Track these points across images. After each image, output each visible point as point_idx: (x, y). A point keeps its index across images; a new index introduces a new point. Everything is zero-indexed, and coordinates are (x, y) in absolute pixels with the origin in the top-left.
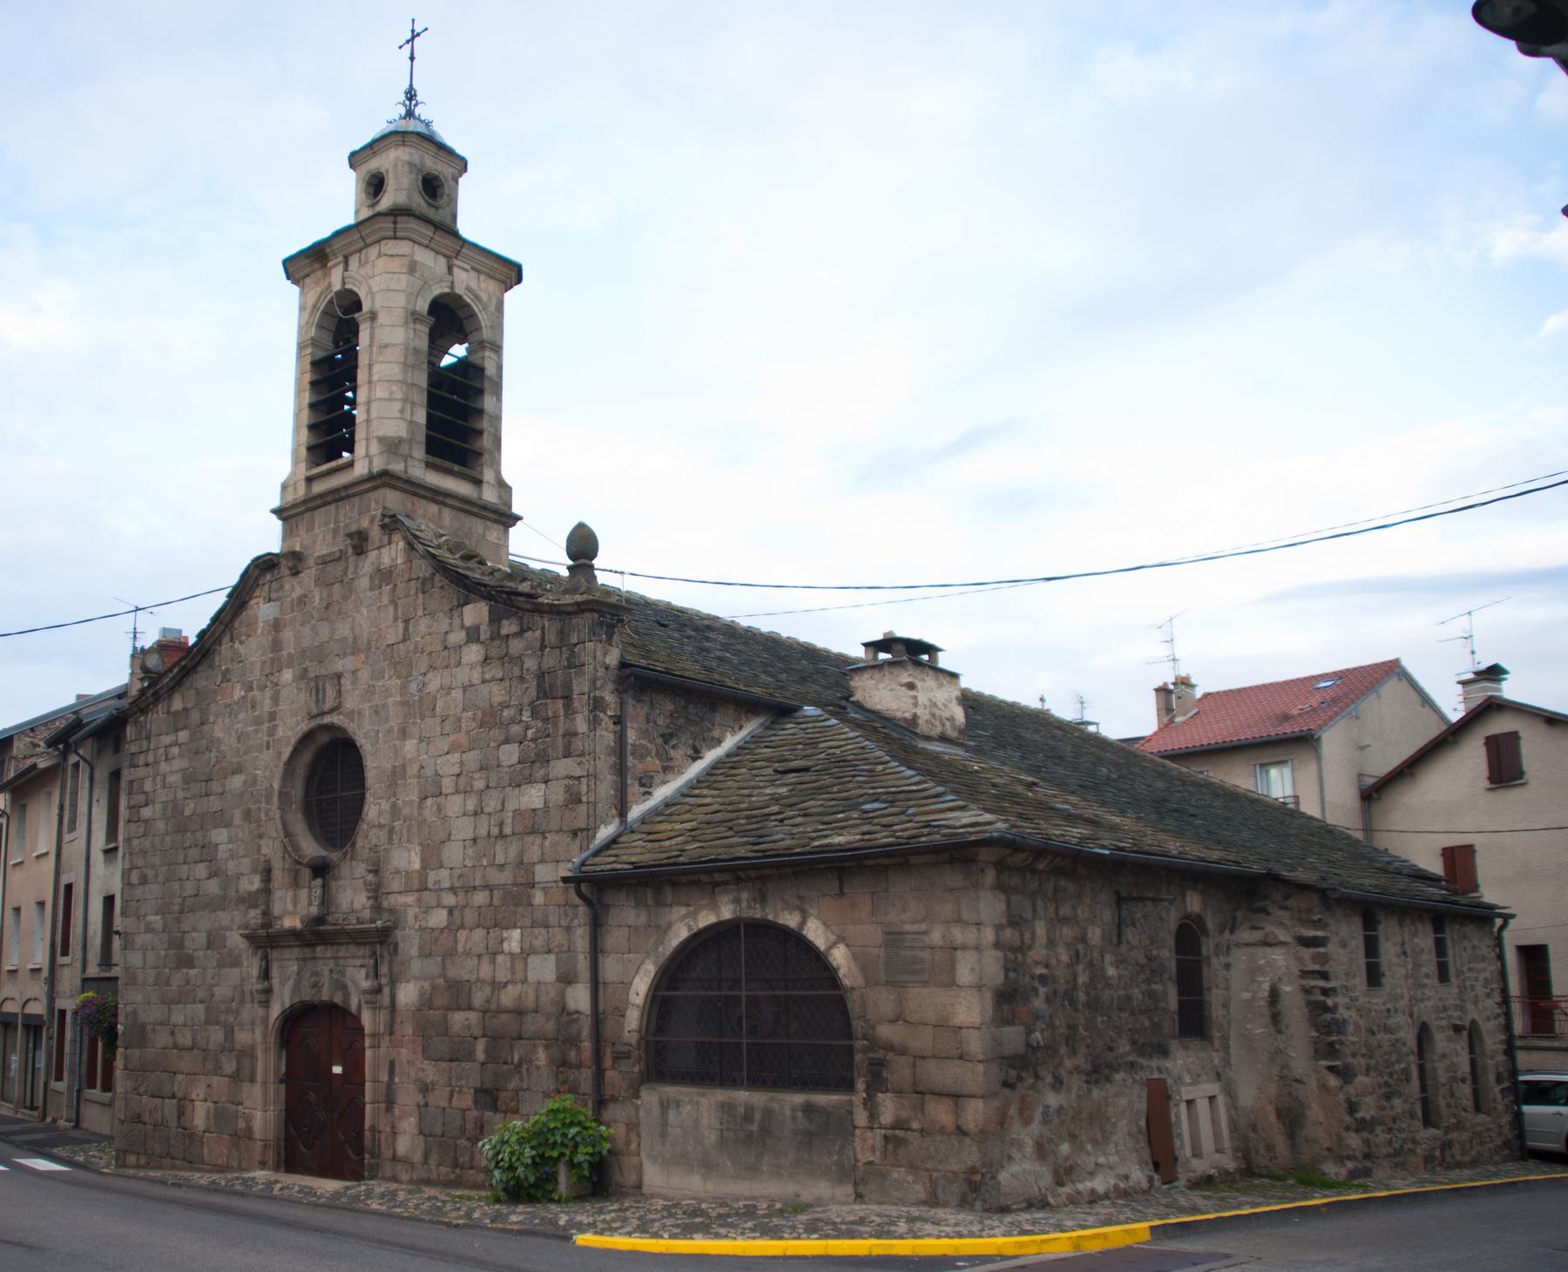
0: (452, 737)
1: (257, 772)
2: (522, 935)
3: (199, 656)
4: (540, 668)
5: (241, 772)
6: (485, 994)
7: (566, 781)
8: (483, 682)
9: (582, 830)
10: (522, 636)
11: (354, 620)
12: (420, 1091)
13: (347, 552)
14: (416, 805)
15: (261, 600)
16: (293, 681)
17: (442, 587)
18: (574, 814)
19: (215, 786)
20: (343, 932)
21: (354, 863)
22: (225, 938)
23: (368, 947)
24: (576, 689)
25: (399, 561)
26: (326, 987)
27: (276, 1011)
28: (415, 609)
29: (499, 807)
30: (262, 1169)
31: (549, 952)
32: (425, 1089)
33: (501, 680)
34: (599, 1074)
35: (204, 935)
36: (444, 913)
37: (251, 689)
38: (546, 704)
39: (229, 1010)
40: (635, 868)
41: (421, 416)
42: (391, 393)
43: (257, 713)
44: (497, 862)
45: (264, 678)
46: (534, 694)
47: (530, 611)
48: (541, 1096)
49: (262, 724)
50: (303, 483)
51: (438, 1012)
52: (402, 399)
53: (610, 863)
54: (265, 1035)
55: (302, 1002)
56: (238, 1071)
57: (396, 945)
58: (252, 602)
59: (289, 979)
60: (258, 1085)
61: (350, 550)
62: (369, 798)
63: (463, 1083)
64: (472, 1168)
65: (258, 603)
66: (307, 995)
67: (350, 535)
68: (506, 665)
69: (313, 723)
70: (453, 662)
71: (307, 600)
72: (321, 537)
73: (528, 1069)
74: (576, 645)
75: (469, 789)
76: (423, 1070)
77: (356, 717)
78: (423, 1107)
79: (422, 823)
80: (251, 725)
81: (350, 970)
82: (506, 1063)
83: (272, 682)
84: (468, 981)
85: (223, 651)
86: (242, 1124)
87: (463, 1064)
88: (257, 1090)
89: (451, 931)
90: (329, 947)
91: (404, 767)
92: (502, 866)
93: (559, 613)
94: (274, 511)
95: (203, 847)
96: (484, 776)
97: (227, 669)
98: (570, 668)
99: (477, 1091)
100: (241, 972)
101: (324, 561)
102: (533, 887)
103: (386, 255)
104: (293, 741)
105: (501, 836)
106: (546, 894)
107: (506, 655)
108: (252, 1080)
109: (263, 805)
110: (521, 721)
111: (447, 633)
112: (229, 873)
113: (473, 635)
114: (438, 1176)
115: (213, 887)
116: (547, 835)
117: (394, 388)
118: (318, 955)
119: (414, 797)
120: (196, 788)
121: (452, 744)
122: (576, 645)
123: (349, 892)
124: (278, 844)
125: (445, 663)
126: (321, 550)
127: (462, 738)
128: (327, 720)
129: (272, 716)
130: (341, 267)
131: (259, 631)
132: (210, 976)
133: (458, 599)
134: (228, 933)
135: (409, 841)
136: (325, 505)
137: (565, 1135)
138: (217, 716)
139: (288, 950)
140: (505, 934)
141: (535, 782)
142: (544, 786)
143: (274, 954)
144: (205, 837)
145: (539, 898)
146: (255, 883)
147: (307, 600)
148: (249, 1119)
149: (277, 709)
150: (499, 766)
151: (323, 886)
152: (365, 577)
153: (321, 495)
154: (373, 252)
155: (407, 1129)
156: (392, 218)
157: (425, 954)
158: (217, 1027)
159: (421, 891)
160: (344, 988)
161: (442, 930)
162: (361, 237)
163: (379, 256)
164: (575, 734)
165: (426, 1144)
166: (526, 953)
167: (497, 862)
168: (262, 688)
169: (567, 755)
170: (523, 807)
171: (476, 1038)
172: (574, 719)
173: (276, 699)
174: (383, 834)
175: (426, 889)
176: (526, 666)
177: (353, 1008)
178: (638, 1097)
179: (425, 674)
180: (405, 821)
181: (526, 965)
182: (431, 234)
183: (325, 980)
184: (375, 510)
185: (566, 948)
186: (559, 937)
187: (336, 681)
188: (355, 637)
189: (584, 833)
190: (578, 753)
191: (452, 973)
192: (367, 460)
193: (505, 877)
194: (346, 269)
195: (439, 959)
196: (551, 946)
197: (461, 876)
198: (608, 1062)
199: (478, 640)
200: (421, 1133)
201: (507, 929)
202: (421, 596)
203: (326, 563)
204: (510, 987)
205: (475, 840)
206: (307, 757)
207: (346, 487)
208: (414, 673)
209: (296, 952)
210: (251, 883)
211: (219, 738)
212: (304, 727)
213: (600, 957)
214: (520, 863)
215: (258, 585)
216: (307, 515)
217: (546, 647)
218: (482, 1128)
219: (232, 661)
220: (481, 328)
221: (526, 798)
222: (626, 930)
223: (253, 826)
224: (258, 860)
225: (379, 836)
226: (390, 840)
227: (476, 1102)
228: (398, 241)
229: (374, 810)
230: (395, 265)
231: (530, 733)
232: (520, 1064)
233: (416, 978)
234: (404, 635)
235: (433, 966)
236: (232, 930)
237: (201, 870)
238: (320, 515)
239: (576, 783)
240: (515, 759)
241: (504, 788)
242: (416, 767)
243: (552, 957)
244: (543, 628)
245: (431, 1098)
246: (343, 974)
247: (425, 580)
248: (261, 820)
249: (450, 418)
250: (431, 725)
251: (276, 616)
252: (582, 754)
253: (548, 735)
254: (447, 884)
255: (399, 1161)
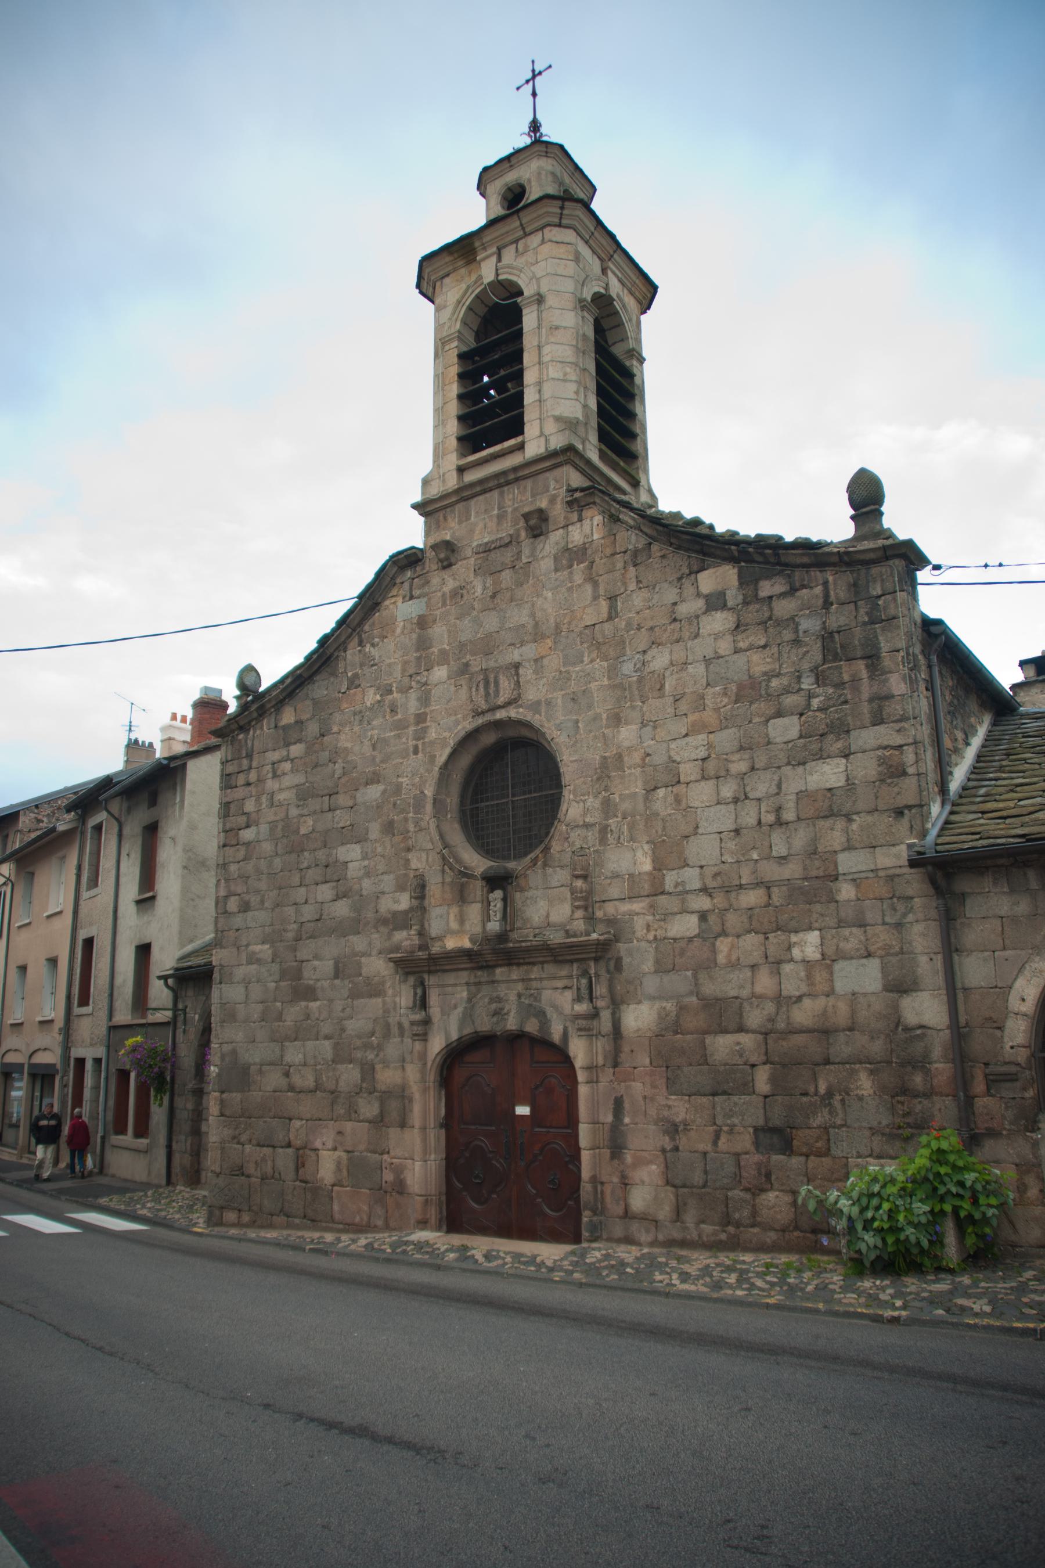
0: (691, 718)
1: (400, 780)
2: (822, 938)
3: (319, 664)
4: (824, 628)
5: (378, 782)
6: (765, 1012)
7: (879, 753)
8: (735, 652)
9: (909, 807)
10: (792, 595)
11: (533, 605)
12: (666, 1132)
13: (518, 536)
14: (640, 799)
15: (400, 600)
16: (449, 678)
17: (663, 557)
18: (896, 789)
19: (343, 800)
20: (528, 950)
21: (549, 870)
22: (359, 965)
23: (575, 965)
24: (885, 646)
25: (596, 536)
26: (512, 1014)
27: (437, 1044)
28: (625, 584)
29: (773, 789)
30: (422, 1229)
31: (869, 955)
32: (673, 1129)
33: (764, 647)
34: (967, 1105)
35: (332, 962)
36: (694, 919)
37: (390, 692)
38: (840, 667)
39: (367, 1046)
40: (1028, 841)
41: (593, 402)
42: (565, 374)
43: (399, 716)
44: (774, 854)
45: (407, 680)
46: (819, 658)
47: (803, 566)
48: (867, 1133)
49: (407, 727)
50: (454, 474)
51: (689, 1037)
52: (576, 381)
53: (972, 841)
54: (423, 1072)
55: (476, 1032)
56: (382, 1115)
57: (619, 961)
58: (387, 602)
59: (455, 1007)
60: (416, 1131)
61: (523, 534)
62: (567, 795)
63: (736, 1121)
64: (753, 1226)
65: (394, 603)
66: (484, 1024)
67: (526, 516)
68: (771, 630)
69: (480, 721)
70: (686, 634)
71: (464, 592)
72: (481, 525)
73: (843, 1101)
74: (879, 597)
75: (723, 773)
76: (670, 1107)
77: (543, 709)
78: (669, 1156)
79: (650, 818)
80: (391, 730)
81: (547, 995)
82: (805, 1094)
83: (418, 682)
84: (736, 998)
85: (349, 657)
86: (388, 1176)
87: (735, 1098)
88: (413, 1138)
89: (705, 939)
90: (515, 967)
91: (619, 757)
92: (783, 859)
93: (848, 564)
94: (415, 506)
95: (327, 866)
96: (746, 756)
97: (356, 676)
98: (873, 623)
99: (756, 1129)
100: (384, 1003)
101: (487, 549)
102: (837, 879)
103: (551, 241)
104: (452, 743)
105: (780, 823)
106: (858, 887)
107: (770, 618)
108: (403, 1124)
109: (411, 815)
110: (800, 690)
111: (675, 604)
112: (364, 893)
113: (716, 602)
114: (700, 1236)
115: (342, 909)
116: (854, 817)
117: (568, 370)
118: (498, 977)
119: (638, 788)
120: (314, 804)
121: (693, 726)
122: (879, 597)
123: (542, 904)
124: (434, 857)
125: (676, 636)
126: (482, 536)
127: (709, 716)
128: (500, 715)
129: (420, 718)
130: (494, 259)
131: (399, 631)
132: (340, 1008)
133: (689, 566)
134: (363, 960)
135: (632, 839)
136: (484, 492)
137: (961, 1184)
138: (342, 725)
139: (453, 974)
140: (794, 938)
141: (829, 757)
142: (844, 761)
143: (431, 980)
144: (329, 855)
145: (846, 892)
146: (404, 902)
147: (464, 592)
148: (398, 1171)
149: (427, 710)
150: (769, 743)
151: (505, 900)
152: (547, 560)
153: (472, 485)
154: (535, 240)
155: (646, 1179)
156: (559, 203)
157: (660, 969)
158: (351, 1066)
159: (656, 895)
160: (541, 1015)
161: (690, 940)
162: (521, 225)
163: (543, 242)
164: (889, 697)
165: (677, 1196)
166: (828, 960)
167: (774, 854)
168: (405, 690)
169: (878, 720)
170: (812, 786)
171: (753, 1066)
172: (886, 680)
173: (425, 699)
174: (592, 836)
175: (662, 893)
176: (801, 628)
177: (556, 1036)
178: (1035, 1129)
179: (644, 652)
180: (624, 818)
181: (831, 974)
182: (592, 229)
183: (512, 1007)
184: (555, 489)
185: (897, 949)
186: (882, 936)
187: (513, 671)
188: (537, 624)
189: (913, 811)
190: (898, 717)
191: (709, 989)
192: (543, 439)
193: (792, 870)
194: (499, 260)
195: (689, 973)
196: (872, 948)
197: (716, 875)
198: (979, 1086)
199: (724, 607)
200: (668, 1183)
201: (796, 932)
202: (632, 569)
203: (490, 550)
204: (807, 1002)
205: (737, 831)
206: (465, 761)
207: (515, 469)
208: (628, 652)
209: (464, 976)
210: (397, 902)
211: (346, 749)
212: (468, 725)
213: (956, 957)
214: (813, 852)
215: (395, 584)
216: (459, 507)
217: (832, 604)
218: (768, 1176)
219: (362, 665)
220: (628, 338)
221: (815, 777)
222: (997, 923)
223: (397, 839)
224: (406, 875)
225: (586, 837)
226: (603, 840)
227: (757, 1144)
228: (562, 229)
229: (572, 809)
230: (561, 251)
231: (815, 703)
232: (830, 1094)
233: (652, 998)
234: (610, 613)
235: (679, 982)
236: (370, 955)
237: (325, 892)
238: (477, 505)
239: (897, 753)
240: (794, 733)
241: (779, 767)
242: (637, 757)
243: (874, 964)
244: (826, 583)
245: (683, 1142)
246: (537, 999)
247: (636, 553)
248: (408, 832)
249: (614, 413)
250: (656, 707)
251: (421, 613)
252: (903, 719)
253: (846, 702)
254: (697, 885)
255: (634, 1217)
